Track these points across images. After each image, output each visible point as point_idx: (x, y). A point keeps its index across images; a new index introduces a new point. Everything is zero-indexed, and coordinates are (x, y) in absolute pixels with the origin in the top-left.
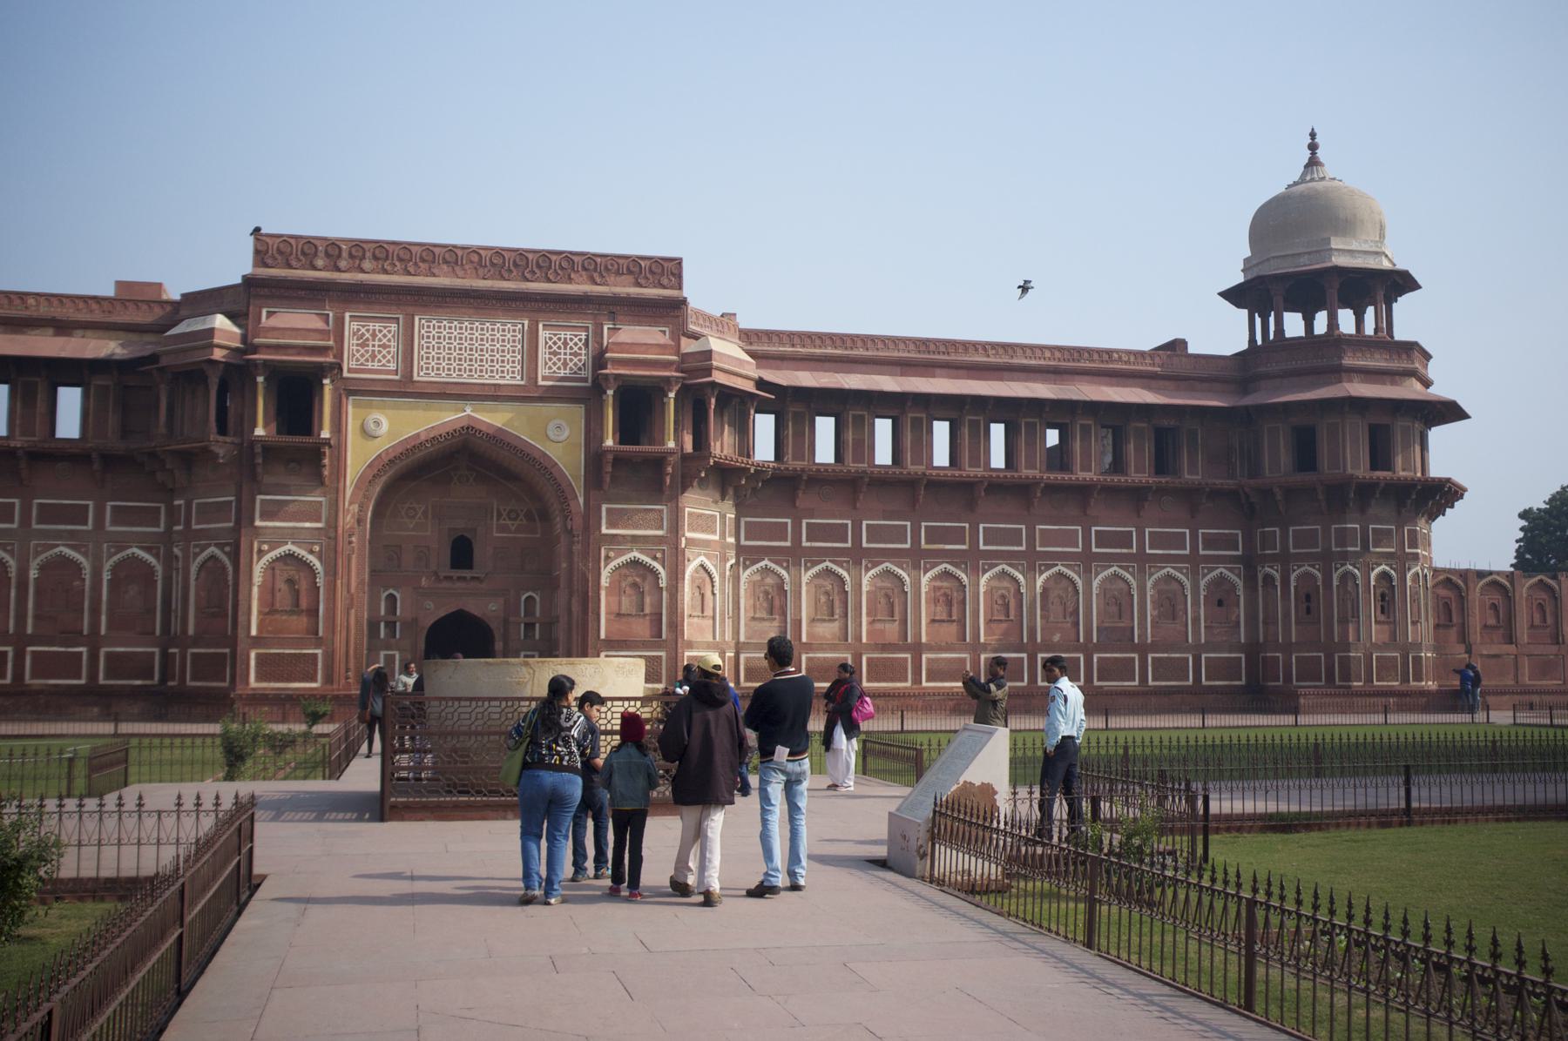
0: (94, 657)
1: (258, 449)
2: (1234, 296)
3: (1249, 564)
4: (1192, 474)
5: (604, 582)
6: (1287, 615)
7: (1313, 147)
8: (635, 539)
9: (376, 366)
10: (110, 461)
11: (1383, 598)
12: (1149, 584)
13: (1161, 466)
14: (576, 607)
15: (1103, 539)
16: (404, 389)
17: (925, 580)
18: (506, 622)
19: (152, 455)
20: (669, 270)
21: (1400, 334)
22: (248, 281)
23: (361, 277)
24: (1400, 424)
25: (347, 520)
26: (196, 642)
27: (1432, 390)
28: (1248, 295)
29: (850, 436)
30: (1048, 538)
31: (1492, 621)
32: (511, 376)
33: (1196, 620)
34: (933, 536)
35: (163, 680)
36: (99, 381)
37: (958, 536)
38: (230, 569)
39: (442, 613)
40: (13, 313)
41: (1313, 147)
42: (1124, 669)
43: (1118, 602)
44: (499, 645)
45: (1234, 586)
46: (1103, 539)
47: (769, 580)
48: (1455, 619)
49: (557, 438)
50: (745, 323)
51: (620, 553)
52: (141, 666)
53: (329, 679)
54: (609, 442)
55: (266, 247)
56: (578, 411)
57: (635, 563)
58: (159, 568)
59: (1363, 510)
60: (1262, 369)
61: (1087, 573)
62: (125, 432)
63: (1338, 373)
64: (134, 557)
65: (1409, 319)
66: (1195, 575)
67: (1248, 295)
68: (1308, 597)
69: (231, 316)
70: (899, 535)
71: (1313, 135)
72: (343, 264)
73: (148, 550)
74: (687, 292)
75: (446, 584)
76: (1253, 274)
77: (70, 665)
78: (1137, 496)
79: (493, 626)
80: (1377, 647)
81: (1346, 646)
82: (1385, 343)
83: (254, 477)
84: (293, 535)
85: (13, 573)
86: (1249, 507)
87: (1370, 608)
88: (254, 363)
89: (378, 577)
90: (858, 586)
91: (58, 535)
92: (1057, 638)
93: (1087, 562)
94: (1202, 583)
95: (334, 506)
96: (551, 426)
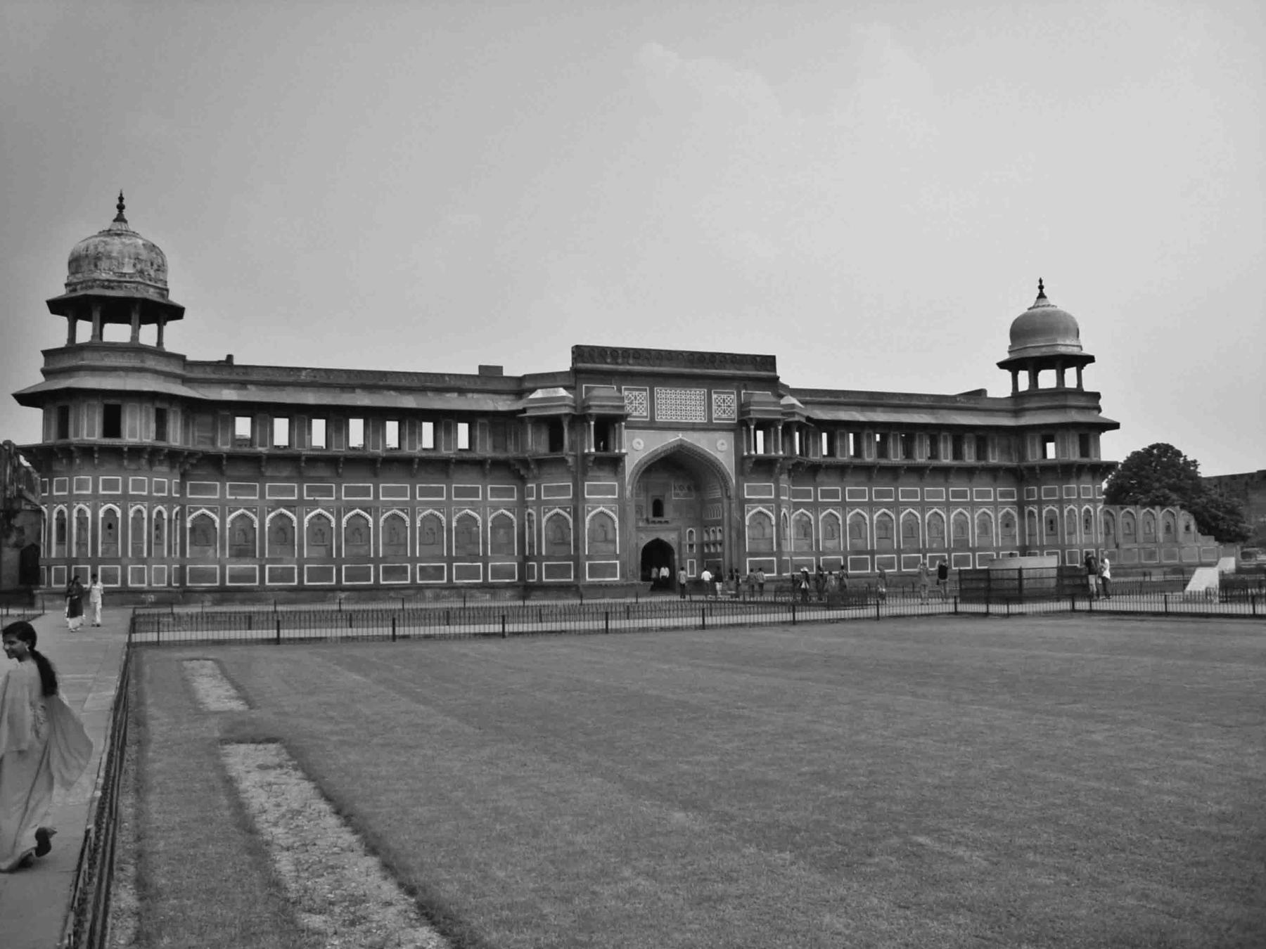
0: (485, 568)
1: (592, 458)
2: (1002, 365)
3: (1021, 505)
4: (994, 459)
5: (747, 523)
6: (1041, 532)
7: (1041, 287)
8: (760, 501)
9: (635, 414)
10: (497, 464)
11: (1087, 522)
13: (979, 458)
14: (734, 535)
15: (955, 494)
16: (652, 425)
17: (875, 517)
19: (525, 463)
20: (768, 362)
21: (1088, 387)
22: (575, 371)
23: (628, 367)
24: (1092, 434)
25: (628, 493)
26: (548, 558)
28: (1012, 366)
29: (838, 443)
30: (930, 495)
32: (700, 419)
33: (997, 535)
34: (880, 494)
35: (520, 579)
36: (480, 421)
37: (888, 494)
38: (571, 520)
39: (650, 540)
40: (440, 386)
41: (1041, 287)
42: (965, 561)
43: (962, 526)
44: (676, 557)
46: (955, 494)
47: (805, 519)
49: (720, 448)
51: (753, 508)
53: (622, 576)
54: (753, 452)
55: (580, 353)
56: (731, 436)
57: (760, 513)
58: (515, 520)
59: (1078, 476)
60: (1026, 406)
61: (948, 512)
62: (495, 448)
63: (1065, 407)
64: (503, 514)
65: (1092, 379)
66: (996, 511)
67: (1012, 366)
68: (1051, 522)
69: (566, 388)
70: (862, 494)
71: (1041, 281)
72: (620, 361)
73: (509, 510)
74: (778, 374)
76: (1016, 356)
77: (474, 573)
78: (969, 472)
79: (675, 546)
80: (1086, 546)
81: (1071, 546)
82: (1079, 391)
83: (585, 473)
86: (1022, 476)
87: (1079, 526)
88: (590, 415)
89: (637, 521)
90: (845, 521)
92: (935, 546)
93: (948, 506)
95: (622, 487)
96: (719, 444)
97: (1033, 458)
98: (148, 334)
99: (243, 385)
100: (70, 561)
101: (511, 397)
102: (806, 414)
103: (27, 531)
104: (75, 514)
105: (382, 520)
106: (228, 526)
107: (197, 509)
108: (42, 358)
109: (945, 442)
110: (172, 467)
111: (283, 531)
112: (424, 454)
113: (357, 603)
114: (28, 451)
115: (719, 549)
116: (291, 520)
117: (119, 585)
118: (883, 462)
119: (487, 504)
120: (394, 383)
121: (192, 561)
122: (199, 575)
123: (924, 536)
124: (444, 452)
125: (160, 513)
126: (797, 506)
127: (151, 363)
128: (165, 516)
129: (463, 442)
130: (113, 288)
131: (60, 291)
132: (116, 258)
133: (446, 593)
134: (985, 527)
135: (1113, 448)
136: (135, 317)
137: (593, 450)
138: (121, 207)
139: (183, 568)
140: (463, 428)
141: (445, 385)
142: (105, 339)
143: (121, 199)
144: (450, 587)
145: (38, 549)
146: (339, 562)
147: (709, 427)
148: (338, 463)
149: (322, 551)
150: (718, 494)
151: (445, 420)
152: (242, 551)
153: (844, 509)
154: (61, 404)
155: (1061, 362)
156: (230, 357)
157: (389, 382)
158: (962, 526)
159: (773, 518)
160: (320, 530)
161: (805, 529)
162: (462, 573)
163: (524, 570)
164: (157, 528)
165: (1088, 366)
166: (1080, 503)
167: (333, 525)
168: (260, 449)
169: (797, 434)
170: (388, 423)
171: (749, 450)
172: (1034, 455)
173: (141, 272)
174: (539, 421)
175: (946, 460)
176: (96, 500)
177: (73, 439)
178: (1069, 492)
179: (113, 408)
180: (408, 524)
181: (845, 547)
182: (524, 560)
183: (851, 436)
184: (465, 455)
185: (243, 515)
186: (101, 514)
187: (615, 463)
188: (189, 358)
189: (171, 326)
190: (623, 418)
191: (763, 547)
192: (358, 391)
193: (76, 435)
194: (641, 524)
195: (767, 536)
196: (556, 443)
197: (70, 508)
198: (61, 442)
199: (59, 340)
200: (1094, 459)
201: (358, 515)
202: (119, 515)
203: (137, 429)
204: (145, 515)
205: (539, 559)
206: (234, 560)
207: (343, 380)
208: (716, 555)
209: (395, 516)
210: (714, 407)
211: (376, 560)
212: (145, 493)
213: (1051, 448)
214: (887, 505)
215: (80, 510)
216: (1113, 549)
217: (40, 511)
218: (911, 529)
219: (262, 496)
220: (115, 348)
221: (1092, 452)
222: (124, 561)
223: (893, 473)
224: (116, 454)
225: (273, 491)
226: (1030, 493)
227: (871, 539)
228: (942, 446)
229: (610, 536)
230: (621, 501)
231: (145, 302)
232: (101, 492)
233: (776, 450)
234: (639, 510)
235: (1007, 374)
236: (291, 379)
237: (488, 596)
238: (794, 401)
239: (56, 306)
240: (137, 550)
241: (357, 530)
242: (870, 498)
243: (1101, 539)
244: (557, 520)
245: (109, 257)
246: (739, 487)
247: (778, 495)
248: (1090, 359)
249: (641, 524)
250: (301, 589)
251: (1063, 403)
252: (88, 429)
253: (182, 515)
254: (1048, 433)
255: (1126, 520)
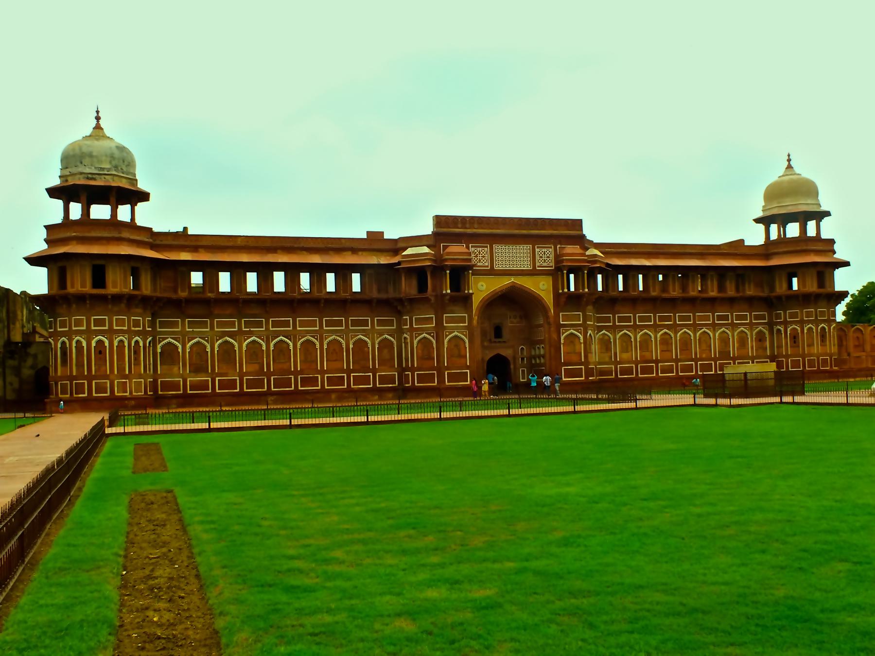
1: (448, 297)
2: (757, 221)
3: (771, 325)
5: (562, 341)
7: (789, 160)
9: (481, 264)
12: (736, 334)
13: (737, 290)
14: (553, 350)
16: (492, 272)
17: (659, 335)
18: (514, 358)
19: (400, 301)
20: (577, 224)
21: (824, 235)
23: (475, 230)
25: (475, 322)
26: (419, 369)
27: (835, 256)
28: (765, 221)
29: (631, 282)
31: (857, 343)
32: (527, 266)
34: (662, 319)
37: (668, 319)
38: (434, 342)
41: (789, 160)
43: (724, 340)
44: (512, 366)
45: (764, 334)
46: (720, 318)
47: (606, 337)
48: (844, 343)
49: (542, 288)
50: (596, 240)
52: (391, 380)
53: (471, 381)
54: (566, 290)
55: (440, 221)
56: (550, 279)
57: (572, 334)
58: (395, 342)
60: (776, 251)
61: (714, 331)
62: (379, 291)
64: (386, 338)
65: (828, 229)
66: (751, 330)
67: (765, 221)
68: (795, 337)
69: (428, 247)
71: (789, 155)
72: (468, 226)
75: (493, 344)
76: (768, 213)
77: (366, 380)
78: (731, 302)
81: (810, 355)
82: (818, 238)
84: (457, 328)
85: (344, 346)
86: (772, 304)
87: (817, 340)
89: (482, 342)
91: (359, 331)
92: (704, 356)
93: (714, 326)
94: (754, 333)
97: (780, 289)
98: (124, 213)
99: (195, 249)
100: (71, 378)
101: (391, 253)
102: (606, 261)
103: (40, 357)
104: (74, 344)
105: (299, 344)
106: (188, 351)
107: (164, 339)
108: (45, 230)
109: (712, 280)
110: (145, 309)
111: (227, 352)
112: (328, 297)
113: (282, 403)
114: (37, 299)
115: (542, 360)
116: (234, 346)
117: (108, 394)
118: (665, 295)
119: (373, 333)
120: (306, 246)
121: (162, 376)
122: (166, 386)
123: (695, 349)
124: (343, 295)
125: (137, 342)
126: (600, 329)
127: (126, 234)
128: (141, 344)
129: (356, 287)
130: (94, 179)
131: (56, 182)
132: (96, 157)
133: (346, 395)
134: (743, 341)
135: (846, 281)
136: (113, 199)
137: (449, 291)
138: (98, 118)
139: (155, 382)
140: (356, 278)
141: (341, 246)
142: (92, 217)
143: (98, 112)
144: (349, 390)
145: (48, 369)
146: (269, 375)
147: (533, 273)
148: (266, 302)
149: (255, 367)
150: (541, 321)
151: (343, 272)
152: (198, 368)
153: (635, 330)
154: (61, 264)
155: (803, 218)
156: (185, 229)
157: (301, 245)
158: (724, 340)
159: (582, 338)
160: (254, 351)
161: (606, 345)
162: (357, 380)
163: (402, 378)
164: (135, 352)
165: (826, 218)
166: (817, 322)
167: (264, 348)
168: (209, 295)
169: (600, 277)
170: (302, 274)
171: (563, 289)
172: (781, 287)
173: (116, 167)
174: (410, 271)
175: (713, 293)
176: (89, 334)
177: (70, 290)
178: (809, 314)
179: (99, 268)
180: (318, 346)
181: (636, 358)
182: (402, 370)
183: (641, 276)
184: (358, 297)
185: (198, 342)
186: (94, 344)
187: (466, 300)
188: (155, 230)
189: (140, 207)
190: (471, 267)
191: (575, 358)
192: (279, 251)
193: (73, 287)
194: (486, 344)
195: (577, 351)
196: (422, 287)
197: (70, 340)
198: (62, 292)
199: (57, 218)
200: (829, 290)
201: (281, 340)
202: (107, 344)
203: (119, 282)
204: (126, 344)
205: (413, 370)
206: (193, 374)
207: (268, 244)
208: (540, 365)
209: (308, 340)
210: (537, 257)
211: (296, 373)
212: (126, 328)
213: (795, 280)
214: (668, 327)
215: (78, 342)
216: (845, 356)
217: (49, 343)
218: (686, 344)
219: (212, 328)
220: (100, 223)
221: (827, 284)
222: (112, 377)
223: (672, 304)
224: (103, 299)
225: (220, 324)
226: (778, 316)
227: (656, 352)
228: (709, 283)
229: (463, 353)
230: (470, 328)
231: (119, 189)
232: (93, 328)
233: (583, 289)
234: (484, 334)
235: (761, 227)
236: (231, 244)
237: (376, 397)
238: (596, 252)
239: (53, 192)
240: (121, 369)
241: (281, 350)
242: (655, 321)
243: (834, 349)
244: (425, 342)
245: (91, 155)
246: (557, 315)
247: (585, 321)
248: (827, 214)
249: (486, 344)
250: (242, 394)
251: (805, 248)
252: (80, 282)
253: (154, 343)
254: (792, 271)
255: (856, 335)
